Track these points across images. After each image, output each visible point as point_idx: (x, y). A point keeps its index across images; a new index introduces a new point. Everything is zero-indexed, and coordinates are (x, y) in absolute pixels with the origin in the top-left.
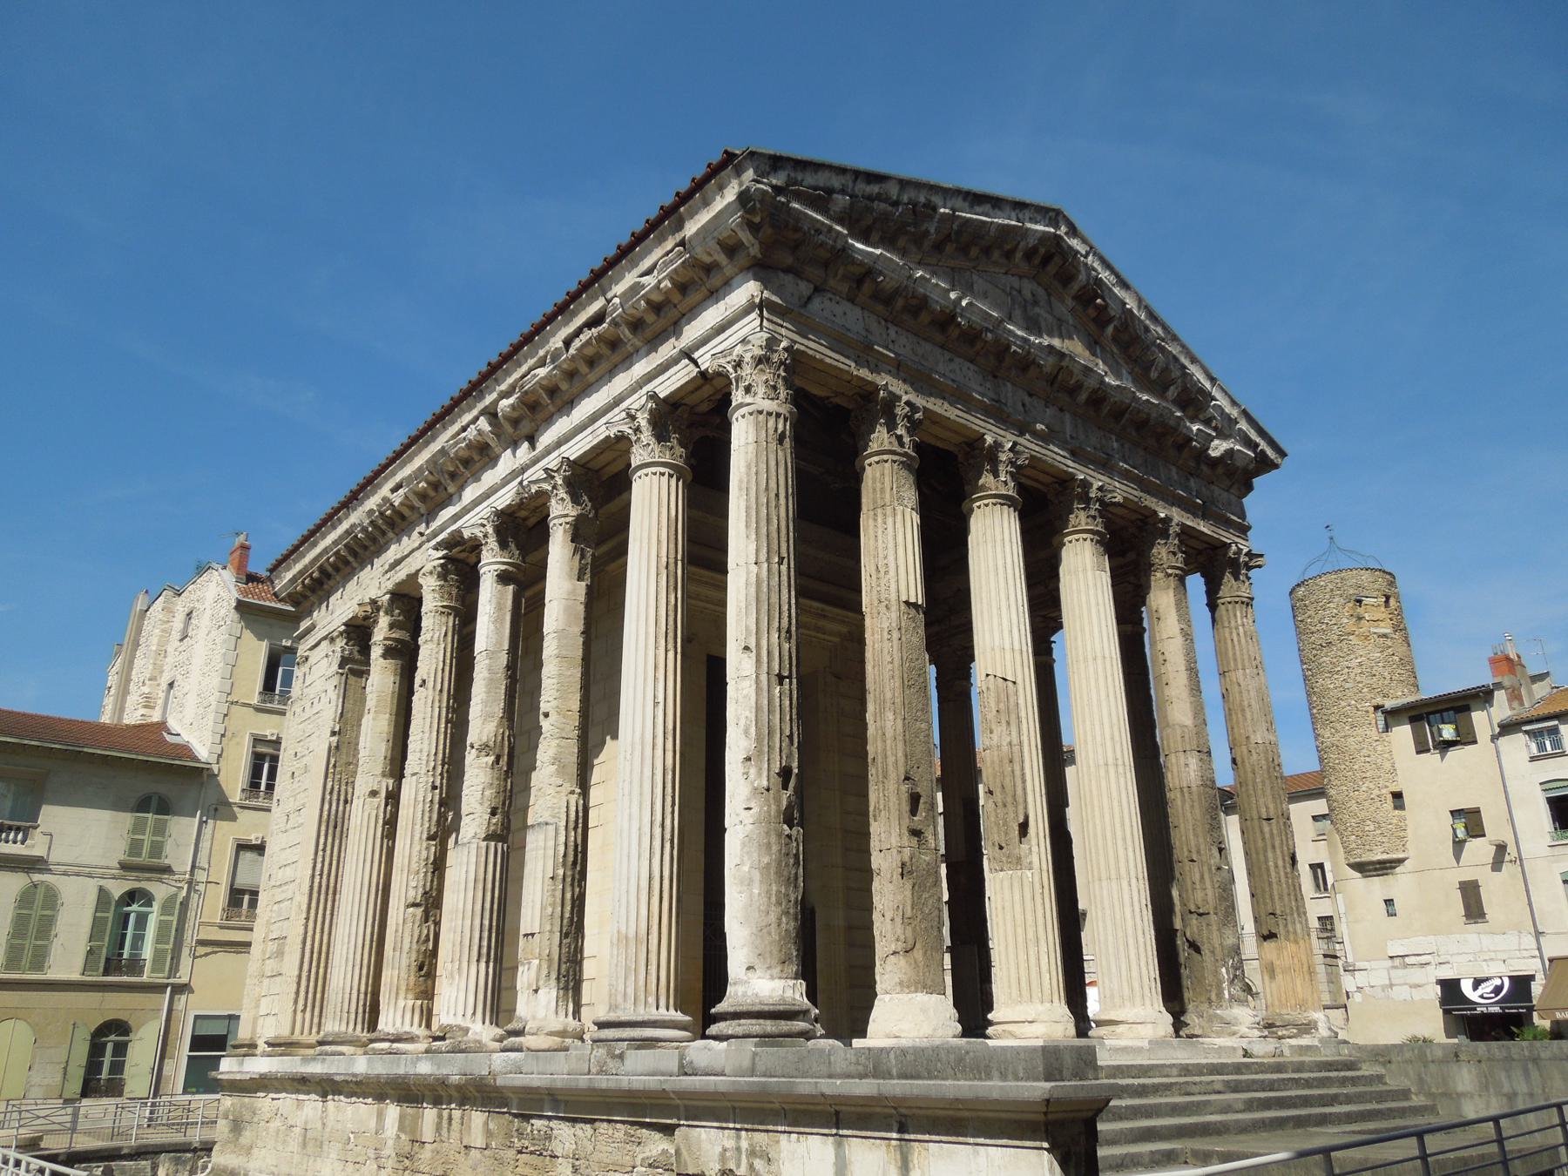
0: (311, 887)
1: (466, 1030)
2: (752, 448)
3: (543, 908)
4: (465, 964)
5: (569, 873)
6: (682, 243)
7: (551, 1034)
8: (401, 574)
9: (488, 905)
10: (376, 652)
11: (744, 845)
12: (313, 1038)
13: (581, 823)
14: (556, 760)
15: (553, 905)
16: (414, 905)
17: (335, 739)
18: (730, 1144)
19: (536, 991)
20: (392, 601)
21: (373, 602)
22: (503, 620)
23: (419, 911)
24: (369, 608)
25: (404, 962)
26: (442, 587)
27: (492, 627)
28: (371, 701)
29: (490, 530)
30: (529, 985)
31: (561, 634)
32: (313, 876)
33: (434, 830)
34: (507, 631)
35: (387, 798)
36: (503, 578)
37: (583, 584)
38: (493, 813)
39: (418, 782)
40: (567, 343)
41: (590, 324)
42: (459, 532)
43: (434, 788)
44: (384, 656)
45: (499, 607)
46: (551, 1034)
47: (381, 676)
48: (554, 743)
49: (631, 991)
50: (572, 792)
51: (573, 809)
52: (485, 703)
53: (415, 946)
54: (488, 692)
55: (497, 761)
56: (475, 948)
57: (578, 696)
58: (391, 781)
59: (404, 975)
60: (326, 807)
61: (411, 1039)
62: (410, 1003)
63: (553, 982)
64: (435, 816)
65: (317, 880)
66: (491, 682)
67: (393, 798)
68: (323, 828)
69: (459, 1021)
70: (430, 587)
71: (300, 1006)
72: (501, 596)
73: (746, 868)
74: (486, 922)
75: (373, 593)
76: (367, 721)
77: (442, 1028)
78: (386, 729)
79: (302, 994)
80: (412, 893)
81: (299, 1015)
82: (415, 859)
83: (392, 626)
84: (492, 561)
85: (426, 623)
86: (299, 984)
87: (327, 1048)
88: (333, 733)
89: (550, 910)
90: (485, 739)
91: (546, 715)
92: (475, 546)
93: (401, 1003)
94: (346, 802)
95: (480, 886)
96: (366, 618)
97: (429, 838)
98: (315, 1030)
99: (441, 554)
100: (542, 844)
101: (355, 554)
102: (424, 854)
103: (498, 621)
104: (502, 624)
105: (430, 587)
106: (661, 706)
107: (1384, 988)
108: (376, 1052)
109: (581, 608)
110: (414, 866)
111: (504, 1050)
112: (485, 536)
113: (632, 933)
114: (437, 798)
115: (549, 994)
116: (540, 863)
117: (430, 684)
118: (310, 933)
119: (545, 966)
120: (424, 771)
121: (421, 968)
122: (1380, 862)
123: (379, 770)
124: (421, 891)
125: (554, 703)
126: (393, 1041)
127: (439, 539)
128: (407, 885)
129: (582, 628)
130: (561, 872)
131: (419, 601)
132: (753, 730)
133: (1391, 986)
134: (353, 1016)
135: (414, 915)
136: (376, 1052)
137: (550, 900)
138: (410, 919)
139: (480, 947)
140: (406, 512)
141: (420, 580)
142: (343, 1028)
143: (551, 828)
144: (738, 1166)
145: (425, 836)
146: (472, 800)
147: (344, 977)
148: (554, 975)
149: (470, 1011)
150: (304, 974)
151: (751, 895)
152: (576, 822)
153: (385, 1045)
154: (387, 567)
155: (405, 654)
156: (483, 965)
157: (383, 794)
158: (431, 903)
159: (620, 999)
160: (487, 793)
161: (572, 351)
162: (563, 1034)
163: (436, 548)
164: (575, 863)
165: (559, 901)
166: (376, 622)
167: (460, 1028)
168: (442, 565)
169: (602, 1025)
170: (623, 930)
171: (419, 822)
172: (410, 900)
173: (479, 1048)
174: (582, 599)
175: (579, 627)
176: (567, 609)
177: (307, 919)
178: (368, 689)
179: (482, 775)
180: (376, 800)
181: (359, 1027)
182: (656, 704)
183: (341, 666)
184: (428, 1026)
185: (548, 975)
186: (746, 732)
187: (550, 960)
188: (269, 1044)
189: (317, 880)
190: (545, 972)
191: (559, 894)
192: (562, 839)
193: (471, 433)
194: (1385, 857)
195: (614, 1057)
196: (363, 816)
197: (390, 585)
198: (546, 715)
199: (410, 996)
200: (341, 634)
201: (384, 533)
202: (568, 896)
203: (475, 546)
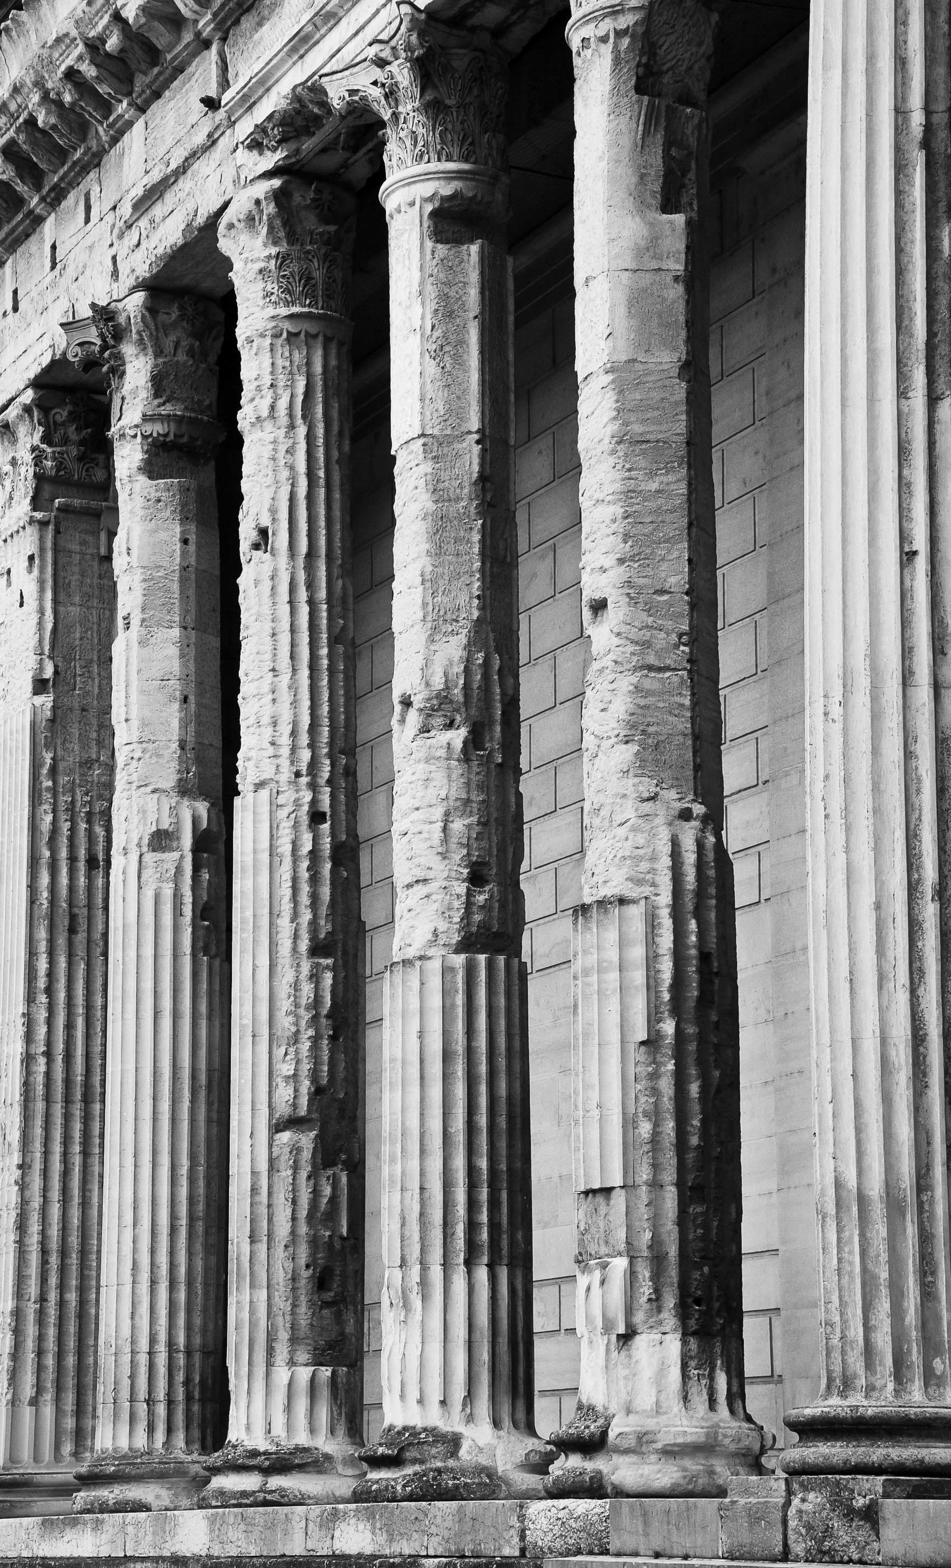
0: (27, 1085)
1: (453, 1442)
3: (629, 1123)
4: (436, 1272)
5: (691, 1030)
7: (670, 1452)
8: (168, 231)
9: (482, 1120)
10: (128, 458)
12: (67, 1472)
13: (708, 899)
14: (637, 729)
15: (655, 1116)
16: (293, 1122)
17: (46, 701)
19: (626, 1338)
20: (151, 309)
21: (104, 313)
22: (462, 343)
23: (307, 1140)
24: (92, 334)
25: (281, 1277)
26: (283, 260)
27: (432, 368)
28: (129, 599)
29: (402, 73)
30: (608, 1327)
31: (623, 374)
32: (28, 1060)
33: (325, 927)
34: (474, 377)
35: (197, 849)
36: (449, 222)
37: (679, 219)
38: (476, 879)
39: (274, 806)
42: (313, 91)
43: (316, 817)
44: (151, 469)
45: (447, 310)
46: (670, 1452)
47: (145, 530)
48: (626, 682)
49: (883, 1341)
50: (686, 815)
51: (690, 858)
52: (430, 582)
53: (303, 1229)
54: (437, 552)
55: (474, 742)
56: (460, 1230)
57: (682, 550)
58: (202, 808)
59: (282, 1304)
60: (44, 879)
62: (304, 1373)
63: (669, 1319)
64: (326, 892)
65: (41, 1066)
66: (440, 525)
67: (214, 849)
68: (42, 934)
69: (434, 1418)
70: (249, 257)
71: (28, 1391)
74: (483, 1163)
75: (101, 290)
76: (124, 648)
77: (394, 1435)
78: (175, 666)
79: (30, 1357)
80: (284, 1093)
81: (27, 1413)
82: (285, 1004)
83: (159, 384)
84: (412, 183)
85: (254, 367)
86: (17, 1332)
87: (109, 1494)
89: (645, 1128)
91: (599, 606)
92: (363, 131)
93: (282, 1375)
94: (92, 863)
95: (460, 1069)
96: (90, 364)
97: (316, 950)
98: (68, 1448)
99: (270, 160)
100: (613, 955)
101: (33, 175)
102: (307, 989)
103: (445, 350)
104: (459, 361)
105: (249, 257)
106: (921, 564)
108: (228, 1500)
109: (676, 293)
110: (285, 1023)
111: (559, 1492)
113: (875, 1187)
114: (326, 844)
115: (661, 1350)
116: (614, 1005)
117: (281, 540)
118: (36, 1202)
119: (644, 1273)
120: (286, 774)
121: (321, 1282)
123: (169, 779)
124: (306, 1085)
125: (618, 574)
128: (265, 1077)
129: (681, 352)
130: (668, 1027)
131: (228, 304)
134: (161, 1410)
135: (296, 1150)
136: (228, 1500)
137: (646, 1102)
138: (285, 1163)
139: (472, 1226)
140: (160, 37)
141: (225, 245)
142: (141, 1441)
143: (636, 912)
145: (304, 945)
146: (420, 846)
147: (129, 1312)
148: (670, 1300)
149: (459, 1392)
150: (31, 1309)
152: (700, 893)
154: (126, 209)
155: (204, 456)
156: (482, 1274)
157: (187, 841)
158: (336, 1121)
159: (857, 1364)
160: (458, 826)
162: (705, 1448)
164: (704, 1000)
165: (667, 1103)
166: (118, 372)
168: (279, 196)
169: (810, 1430)
170: (851, 1181)
171: (286, 907)
172: (283, 1110)
173: (487, 1485)
174: (678, 266)
175: (668, 358)
176: (639, 303)
177: (23, 1167)
178: (119, 562)
179: (439, 778)
180: (176, 855)
181: (180, 1439)
182: (907, 557)
183: (36, 503)
184: (355, 1431)
185: (656, 1300)
187: (658, 1260)
189: (41, 1066)
190: (646, 1289)
191: (666, 1085)
192: (666, 940)
195: (850, 1514)
196: (141, 900)
197: (140, 265)
198: (599, 606)
199: (303, 1356)
200: (27, 409)
201: (106, 107)
202: (694, 1089)
203: (363, 131)
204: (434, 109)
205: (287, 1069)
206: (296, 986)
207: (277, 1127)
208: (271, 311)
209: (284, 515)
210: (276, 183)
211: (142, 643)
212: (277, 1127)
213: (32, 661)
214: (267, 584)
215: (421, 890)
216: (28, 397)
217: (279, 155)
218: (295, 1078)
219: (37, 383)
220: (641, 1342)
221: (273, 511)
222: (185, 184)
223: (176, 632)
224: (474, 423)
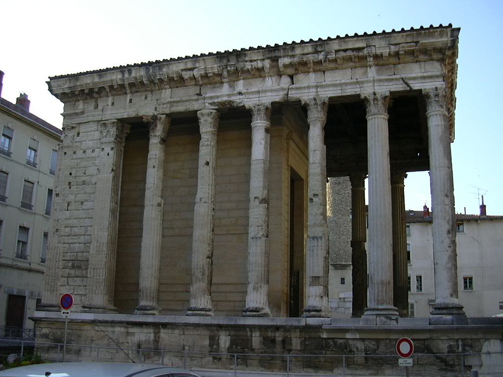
2: (443, 127)
6: (417, 43)
11: (449, 258)
18: (452, 343)
40: (337, 51)
41: (353, 50)
61: (209, 310)
69: (261, 306)
72: (266, 137)
73: (450, 265)
88: (113, 170)
90: (264, 196)
107: (336, 309)
112: (259, 110)
117: (211, 164)
120: (210, 202)
122: (343, 265)
125: (321, 192)
126: (206, 311)
127: (216, 101)
132: (451, 223)
133: (338, 308)
144: (458, 349)
151: (452, 273)
153: (203, 312)
161: (337, 55)
163: (211, 104)
167: (263, 309)
180: (160, 208)
183: (115, 139)
186: (448, 222)
188: (84, 307)
193: (260, 64)
194: (345, 263)
200: (114, 123)
204: (266, 114)
205: (209, 249)
206: (210, 236)
207: (207, 258)
208: (211, 129)
209: (211, 161)
210: (215, 111)
211: (157, 171)
212: (207, 258)
213: (112, 166)
214: (208, 171)
215: (261, 227)
216: (116, 120)
217: (216, 107)
218: (209, 251)
219: (117, 119)
220: (324, 297)
221: (210, 160)
222: (187, 103)
223: (162, 170)
224: (268, 159)
